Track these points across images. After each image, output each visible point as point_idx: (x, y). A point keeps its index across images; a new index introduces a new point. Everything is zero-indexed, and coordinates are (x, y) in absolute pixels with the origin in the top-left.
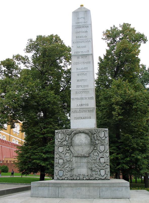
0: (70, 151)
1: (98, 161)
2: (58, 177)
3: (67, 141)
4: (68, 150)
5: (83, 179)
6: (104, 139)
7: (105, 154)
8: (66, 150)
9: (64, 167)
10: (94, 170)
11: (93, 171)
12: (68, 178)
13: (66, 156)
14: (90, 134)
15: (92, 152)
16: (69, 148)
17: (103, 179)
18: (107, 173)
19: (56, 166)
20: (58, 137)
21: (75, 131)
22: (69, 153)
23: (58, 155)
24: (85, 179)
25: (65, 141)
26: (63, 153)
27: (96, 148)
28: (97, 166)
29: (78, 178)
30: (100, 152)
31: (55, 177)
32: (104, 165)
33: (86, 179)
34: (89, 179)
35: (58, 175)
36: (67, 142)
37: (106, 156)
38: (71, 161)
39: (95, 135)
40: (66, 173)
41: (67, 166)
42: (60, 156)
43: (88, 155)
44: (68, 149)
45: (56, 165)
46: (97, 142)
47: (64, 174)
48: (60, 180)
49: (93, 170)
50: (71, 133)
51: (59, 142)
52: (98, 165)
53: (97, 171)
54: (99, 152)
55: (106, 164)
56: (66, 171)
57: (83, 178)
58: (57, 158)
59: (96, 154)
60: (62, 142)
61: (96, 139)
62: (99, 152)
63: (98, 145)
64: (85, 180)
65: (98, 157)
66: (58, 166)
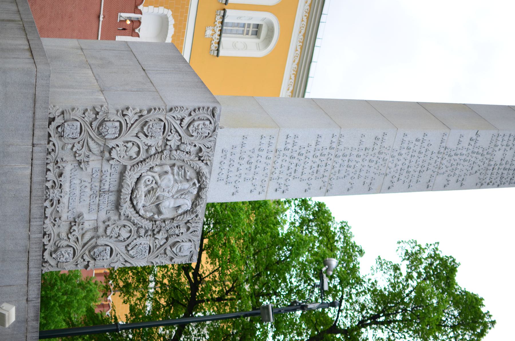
0: (144, 157)
2: (59, 121)
4: (147, 151)
6: (165, 253)
7: (121, 260)
9: (90, 140)
10: (74, 231)
12: (52, 154)
13: (130, 145)
16: (155, 155)
19: (97, 113)
20: (196, 118)
21: (205, 170)
23: (136, 117)
25: (181, 139)
26: (141, 135)
27: (142, 232)
32: (87, 258)
33: (46, 207)
34: (46, 218)
36: (174, 147)
37: (114, 261)
39: (183, 230)
40: (70, 146)
41: (92, 150)
42: (132, 125)
43: (122, 214)
44: (153, 151)
45: (100, 114)
46: (161, 237)
50: (202, 161)
53: (69, 238)
54: (130, 243)
55: (88, 262)
56: (77, 147)
58: (124, 115)
59: (124, 234)
60: (177, 131)
62: (130, 243)
63: (153, 239)
65: (114, 239)
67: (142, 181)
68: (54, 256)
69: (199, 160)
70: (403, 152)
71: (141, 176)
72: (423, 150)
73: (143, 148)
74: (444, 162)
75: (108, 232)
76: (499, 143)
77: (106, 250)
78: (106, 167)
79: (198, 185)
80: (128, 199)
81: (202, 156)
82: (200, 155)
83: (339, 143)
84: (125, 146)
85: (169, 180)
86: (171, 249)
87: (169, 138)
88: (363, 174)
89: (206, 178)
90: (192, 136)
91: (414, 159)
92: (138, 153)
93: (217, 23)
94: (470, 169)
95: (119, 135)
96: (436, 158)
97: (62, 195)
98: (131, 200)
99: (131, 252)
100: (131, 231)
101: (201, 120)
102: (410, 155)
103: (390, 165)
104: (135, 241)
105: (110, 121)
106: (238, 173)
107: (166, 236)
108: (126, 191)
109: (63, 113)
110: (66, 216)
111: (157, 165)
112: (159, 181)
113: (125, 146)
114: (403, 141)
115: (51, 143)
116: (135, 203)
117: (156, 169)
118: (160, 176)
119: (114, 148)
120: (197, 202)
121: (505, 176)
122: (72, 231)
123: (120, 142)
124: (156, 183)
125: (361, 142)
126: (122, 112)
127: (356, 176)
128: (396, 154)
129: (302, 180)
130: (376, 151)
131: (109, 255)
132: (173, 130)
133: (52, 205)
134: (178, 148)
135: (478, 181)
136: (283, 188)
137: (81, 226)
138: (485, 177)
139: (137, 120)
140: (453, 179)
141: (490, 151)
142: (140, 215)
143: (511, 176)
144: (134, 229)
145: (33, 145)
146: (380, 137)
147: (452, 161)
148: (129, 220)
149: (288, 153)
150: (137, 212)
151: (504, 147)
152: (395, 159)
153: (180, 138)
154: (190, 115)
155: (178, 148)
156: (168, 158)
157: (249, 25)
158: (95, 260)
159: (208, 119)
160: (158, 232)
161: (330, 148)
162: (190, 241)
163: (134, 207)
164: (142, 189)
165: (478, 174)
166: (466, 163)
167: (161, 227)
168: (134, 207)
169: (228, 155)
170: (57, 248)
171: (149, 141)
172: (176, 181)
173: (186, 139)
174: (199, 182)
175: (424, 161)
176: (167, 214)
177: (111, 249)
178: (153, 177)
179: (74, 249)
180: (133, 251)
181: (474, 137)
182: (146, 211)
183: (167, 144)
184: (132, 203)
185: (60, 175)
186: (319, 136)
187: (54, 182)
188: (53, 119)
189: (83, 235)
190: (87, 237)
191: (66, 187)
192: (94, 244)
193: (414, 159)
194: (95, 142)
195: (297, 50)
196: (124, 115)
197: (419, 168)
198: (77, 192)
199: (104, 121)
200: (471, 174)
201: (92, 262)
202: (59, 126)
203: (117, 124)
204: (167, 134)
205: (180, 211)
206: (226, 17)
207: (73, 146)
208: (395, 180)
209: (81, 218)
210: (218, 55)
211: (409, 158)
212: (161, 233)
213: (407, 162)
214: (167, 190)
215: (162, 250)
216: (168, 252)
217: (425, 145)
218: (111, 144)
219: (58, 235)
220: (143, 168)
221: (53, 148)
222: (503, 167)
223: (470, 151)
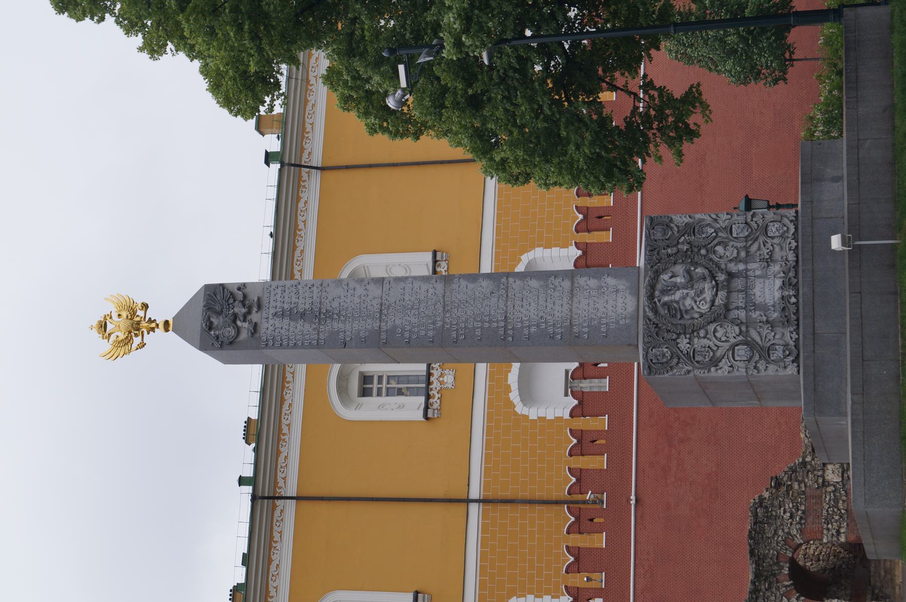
3: (678, 338)
4: (707, 333)
5: (794, 286)
9: (760, 343)
11: (770, 258)
13: (724, 339)
19: (755, 367)
21: (650, 314)
22: (715, 329)
24: (796, 280)
26: (715, 348)
29: (793, 300)
33: (795, 277)
34: (794, 267)
40: (777, 336)
45: (753, 368)
47: (781, 342)
48: (798, 355)
50: (654, 323)
52: (754, 242)
53: (772, 245)
55: (752, 220)
57: (791, 287)
61: (675, 250)
64: (798, 281)
66: (756, 363)
68: (785, 228)
69: (657, 324)
73: (710, 336)
75: (735, 251)
77: (737, 234)
79: (656, 300)
81: (655, 328)
84: (728, 337)
86: (673, 233)
87: (688, 345)
89: (649, 307)
92: (715, 331)
94: (342, 304)
101: (660, 363)
105: (744, 361)
109: (785, 367)
111: (697, 319)
112: (693, 304)
113: (728, 337)
115: (794, 340)
118: (692, 308)
119: (738, 336)
120: (654, 282)
122: (770, 253)
123: (733, 341)
124: (696, 302)
126: (733, 369)
131: (733, 230)
133: (790, 279)
135: (328, 290)
138: (320, 294)
139: (720, 362)
143: (286, 295)
145: (814, 351)
153: (678, 346)
154: (671, 367)
158: (746, 223)
159: (654, 364)
162: (655, 240)
165: (330, 298)
167: (686, 257)
170: (781, 236)
174: (655, 303)
177: (731, 235)
179: (767, 234)
180: (711, 232)
183: (689, 339)
185: (784, 309)
188: (793, 361)
189: (759, 249)
194: (755, 341)
196: (731, 366)
198: (767, 290)
199: (749, 361)
200: (339, 297)
201: (749, 220)
202: (788, 355)
203: (737, 358)
204: (690, 350)
207: (774, 336)
209: (763, 266)
210: (435, 253)
219: (782, 249)
221: (792, 335)
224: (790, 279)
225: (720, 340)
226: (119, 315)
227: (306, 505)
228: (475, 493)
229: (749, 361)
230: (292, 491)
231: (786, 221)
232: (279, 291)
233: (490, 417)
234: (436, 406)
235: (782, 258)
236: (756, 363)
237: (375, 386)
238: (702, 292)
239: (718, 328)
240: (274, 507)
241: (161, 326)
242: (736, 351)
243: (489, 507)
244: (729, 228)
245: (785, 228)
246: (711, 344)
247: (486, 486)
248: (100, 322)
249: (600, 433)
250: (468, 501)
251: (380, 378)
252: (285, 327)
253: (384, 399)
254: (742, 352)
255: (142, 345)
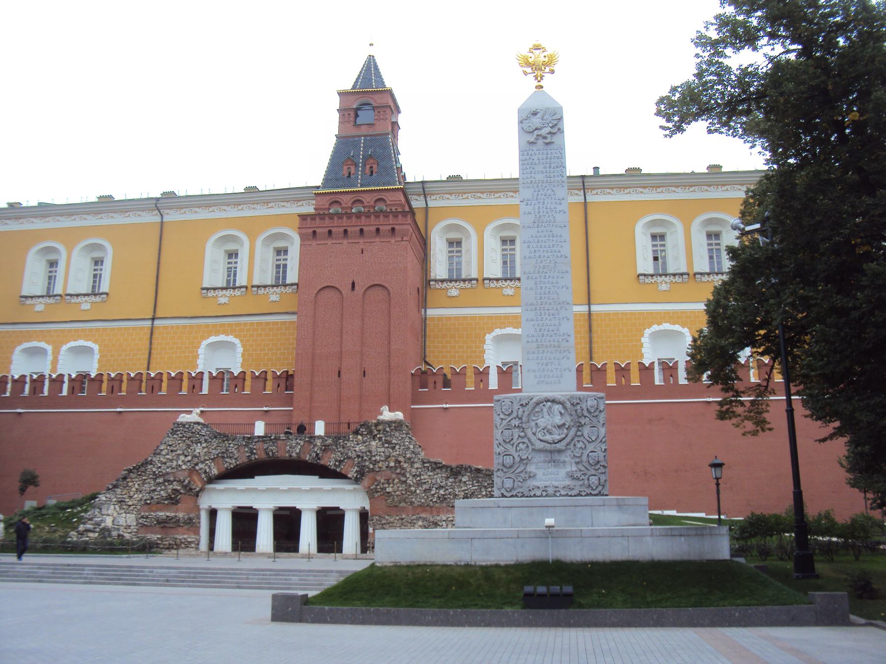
0: (526, 439)
1: (584, 458)
2: (503, 491)
3: (519, 419)
6: (597, 416)
7: (600, 444)
8: (519, 436)
9: (515, 472)
10: (577, 476)
13: (518, 448)
14: (568, 405)
15: (572, 440)
17: (595, 495)
18: (602, 481)
21: (534, 400)
23: (501, 447)
24: (558, 495)
25: (515, 418)
26: (512, 443)
27: (579, 433)
28: (583, 468)
29: (544, 494)
30: (589, 442)
31: (496, 493)
34: (567, 494)
35: (503, 487)
36: (520, 421)
38: (530, 458)
39: (578, 407)
40: (520, 483)
44: (522, 434)
45: (499, 468)
46: (583, 421)
47: (516, 486)
48: (507, 497)
49: (575, 477)
51: (504, 421)
52: (585, 467)
53: (583, 479)
56: (520, 479)
59: (580, 445)
60: (510, 421)
64: (557, 496)
65: (584, 451)
66: (502, 470)
67: (541, 438)
70: (537, 254)
71: (539, 439)
72: (536, 240)
73: (520, 440)
74: (545, 220)
75: (579, 455)
76: (529, 180)
78: (535, 460)
79: (545, 403)
80: (554, 445)
82: (524, 404)
83: (532, 304)
85: (541, 421)
87: (513, 425)
88: (555, 280)
90: (512, 411)
91: (543, 244)
92: (523, 443)
93: (710, 279)
95: (510, 455)
96: (543, 228)
97: (551, 485)
98: (556, 443)
99: (593, 439)
100: (578, 441)
102: (540, 249)
103: (548, 262)
104: (586, 437)
106: (554, 371)
107: (583, 417)
108: (548, 447)
109: (499, 489)
110: (568, 482)
112: (542, 428)
114: (530, 258)
116: (556, 441)
117: (534, 430)
118: (539, 427)
121: (555, 165)
124: (543, 429)
125: (532, 289)
127: (557, 285)
128: (539, 260)
129: (560, 325)
130: (537, 275)
131: (594, 453)
132: (509, 423)
133: (559, 491)
134: (521, 419)
135: (560, 186)
136: (566, 336)
137: (574, 473)
140: (559, 208)
141: (535, 185)
142: (566, 436)
143: (556, 160)
144: (576, 439)
145: (499, 507)
146: (527, 275)
147: (545, 214)
148: (570, 443)
149: (539, 339)
150: (564, 438)
151: (532, 175)
152: (543, 259)
154: (499, 415)
155: (521, 419)
156: (528, 424)
157: (709, 245)
158: (598, 462)
160: (581, 423)
161: (536, 309)
163: (560, 441)
164: (548, 437)
165: (554, 189)
166: (546, 202)
168: (560, 441)
169: (541, 380)
170: (589, 486)
171: (516, 436)
172: (543, 417)
173: (514, 415)
175: (545, 236)
176: (567, 419)
178: (539, 432)
181: (525, 203)
182: (562, 434)
183: (518, 426)
184: (558, 442)
185: (539, 488)
186: (527, 320)
187: (543, 491)
188: (502, 494)
189: (580, 471)
190: (583, 468)
191: (547, 484)
192: (588, 463)
193: (543, 244)
195: (727, 190)
196: (499, 454)
197: (551, 238)
199: (503, 465)
200: (554, 195)
201: (601, 463)
203: (505, 457)
205: (563, 411)
206: (703, 271)
207: (520, 481)
208: (559, 254)
211: (542, 249)
212: (581, 421)
213: (545, 249)
214: (548, 422)
215: (594, 419)
216: (595, 414)
217: (531, 239)
218: (517, 459)
219: (581, 486)
220: (533, 438)
222: (548, 170)
223: (536, 202)
224: (559, 491)
225: (517, 446)
226: (545, 56)
227: (582, 208)
228: (594, 308)
229: (503, 465)
230: (589, 199)
231: (600, 488)
232: (559, 155)
233: (641, 314)
234: (647, 280)
235: (575, 486)
236: (502, 470)
237: (659, 243)
238: (551, 434)
239: (526, 445)
240: (579, 190)
241: (539, 84)
242: (508, 457)
243: (586, 317)
244: (595, 450)
245: (594, 488)
246: (514, 441)
247: (599, 314)
248: (540, 45)
249: (628, 381)
250: (589, 304)
251: (664, 245)
252: (534, 161)
253: (650, 249)
254: (508, 460)
255: (525, 73)
